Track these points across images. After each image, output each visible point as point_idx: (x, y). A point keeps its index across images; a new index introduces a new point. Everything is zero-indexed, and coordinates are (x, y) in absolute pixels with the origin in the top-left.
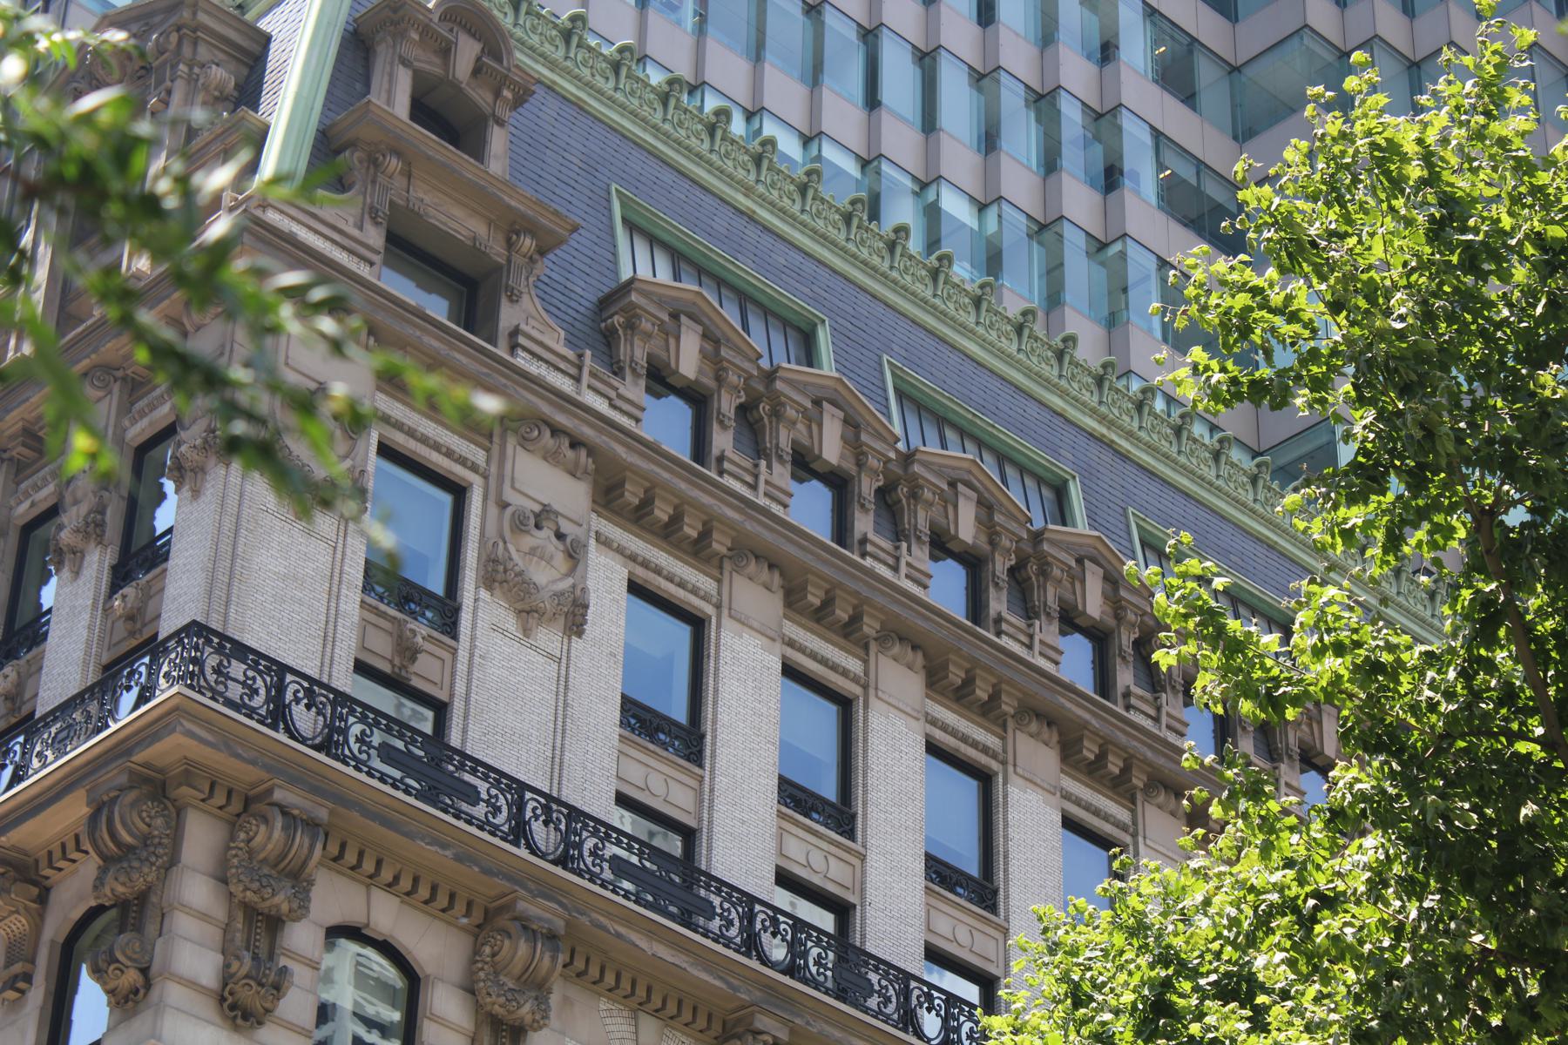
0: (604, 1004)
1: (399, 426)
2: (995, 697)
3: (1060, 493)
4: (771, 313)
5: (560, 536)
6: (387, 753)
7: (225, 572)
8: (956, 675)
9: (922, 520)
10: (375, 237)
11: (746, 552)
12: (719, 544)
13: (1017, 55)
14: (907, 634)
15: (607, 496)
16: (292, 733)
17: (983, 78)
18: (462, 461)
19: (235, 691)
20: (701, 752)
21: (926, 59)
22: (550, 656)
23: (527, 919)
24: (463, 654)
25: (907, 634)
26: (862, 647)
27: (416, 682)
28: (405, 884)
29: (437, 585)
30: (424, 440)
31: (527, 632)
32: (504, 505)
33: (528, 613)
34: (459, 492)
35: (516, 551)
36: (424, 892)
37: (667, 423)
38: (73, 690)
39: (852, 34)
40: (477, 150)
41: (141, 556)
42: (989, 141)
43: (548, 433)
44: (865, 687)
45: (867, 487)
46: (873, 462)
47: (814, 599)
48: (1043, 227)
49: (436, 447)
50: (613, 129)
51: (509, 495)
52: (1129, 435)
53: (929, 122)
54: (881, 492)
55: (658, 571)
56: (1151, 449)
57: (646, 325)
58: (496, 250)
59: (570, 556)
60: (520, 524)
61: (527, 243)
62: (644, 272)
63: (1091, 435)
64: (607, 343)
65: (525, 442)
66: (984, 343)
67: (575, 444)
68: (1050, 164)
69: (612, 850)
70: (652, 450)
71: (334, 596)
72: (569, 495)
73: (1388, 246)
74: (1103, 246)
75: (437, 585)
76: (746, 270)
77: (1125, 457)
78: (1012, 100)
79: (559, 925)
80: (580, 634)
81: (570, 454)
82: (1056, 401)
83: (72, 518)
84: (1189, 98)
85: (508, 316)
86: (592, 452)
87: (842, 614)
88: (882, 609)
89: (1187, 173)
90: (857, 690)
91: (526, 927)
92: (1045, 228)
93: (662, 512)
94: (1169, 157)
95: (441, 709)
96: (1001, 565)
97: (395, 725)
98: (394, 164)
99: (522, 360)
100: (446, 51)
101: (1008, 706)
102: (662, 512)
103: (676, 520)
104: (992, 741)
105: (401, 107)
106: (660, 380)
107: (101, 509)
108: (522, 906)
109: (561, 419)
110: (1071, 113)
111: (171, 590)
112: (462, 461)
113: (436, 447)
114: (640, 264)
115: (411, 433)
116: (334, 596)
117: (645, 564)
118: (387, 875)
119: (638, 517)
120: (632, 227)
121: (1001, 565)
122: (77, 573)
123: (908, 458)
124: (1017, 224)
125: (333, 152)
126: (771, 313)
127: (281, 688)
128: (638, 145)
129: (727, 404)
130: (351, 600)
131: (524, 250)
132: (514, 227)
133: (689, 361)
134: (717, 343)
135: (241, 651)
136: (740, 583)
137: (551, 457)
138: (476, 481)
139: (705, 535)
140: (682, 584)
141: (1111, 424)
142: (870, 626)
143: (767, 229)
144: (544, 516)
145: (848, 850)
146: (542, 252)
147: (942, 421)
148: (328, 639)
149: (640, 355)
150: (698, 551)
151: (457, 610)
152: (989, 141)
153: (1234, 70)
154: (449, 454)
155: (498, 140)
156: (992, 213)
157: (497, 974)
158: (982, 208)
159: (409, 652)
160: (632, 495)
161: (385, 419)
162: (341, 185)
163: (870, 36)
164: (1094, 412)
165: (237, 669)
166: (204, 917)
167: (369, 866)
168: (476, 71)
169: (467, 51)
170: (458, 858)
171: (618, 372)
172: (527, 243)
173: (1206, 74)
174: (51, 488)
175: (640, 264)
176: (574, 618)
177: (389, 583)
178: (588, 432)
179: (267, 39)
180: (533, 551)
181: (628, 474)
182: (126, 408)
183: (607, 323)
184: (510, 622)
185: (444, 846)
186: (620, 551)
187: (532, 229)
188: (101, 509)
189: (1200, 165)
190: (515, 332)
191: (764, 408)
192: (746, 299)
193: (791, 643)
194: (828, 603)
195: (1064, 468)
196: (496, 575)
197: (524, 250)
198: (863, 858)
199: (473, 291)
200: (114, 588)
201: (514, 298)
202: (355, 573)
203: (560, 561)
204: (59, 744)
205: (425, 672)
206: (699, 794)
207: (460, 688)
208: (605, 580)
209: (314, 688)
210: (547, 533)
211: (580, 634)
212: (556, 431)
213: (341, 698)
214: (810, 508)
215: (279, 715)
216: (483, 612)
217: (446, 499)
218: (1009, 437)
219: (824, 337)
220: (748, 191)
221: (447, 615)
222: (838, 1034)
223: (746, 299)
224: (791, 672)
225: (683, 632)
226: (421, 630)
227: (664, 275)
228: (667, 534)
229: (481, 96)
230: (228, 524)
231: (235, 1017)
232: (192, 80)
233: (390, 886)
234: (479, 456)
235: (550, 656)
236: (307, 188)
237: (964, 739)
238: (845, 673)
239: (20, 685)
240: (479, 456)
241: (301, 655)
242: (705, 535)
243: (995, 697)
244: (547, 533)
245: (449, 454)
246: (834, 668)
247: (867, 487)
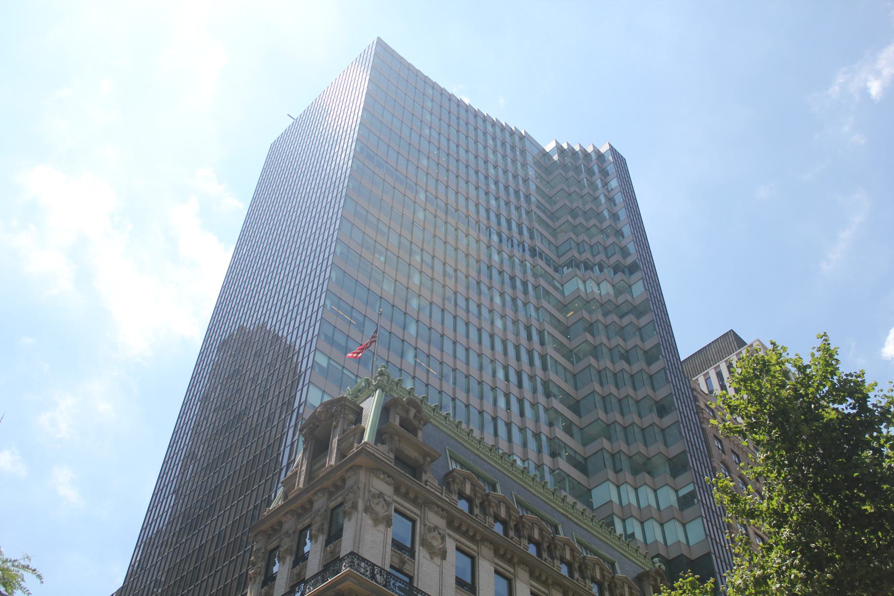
1: (399, 504)
2: (547, 579)
3: (556, 528)
4: (485, 480)
6: (400, 588)
7: (358, 539)
8: (537, 573)
9: (526, 533)
10: (392, 456)
11: (485, 540)
13: (530, 424)
14: (524, 562)
15: (450, 524)
16: (376, 582)
17: (522, 430)
18: (415, 513)
19: (362, 570)
21: (508, 425)
24: (416, 564)
25: (524, 562)
26: (513, 565)
29: (408, 545)
30: (405, 508)
31: (432, 558)
32: (425, 525)
33: (432, 553)
34: (414, 522)
35: (429, 537)
37: (463, 505)
38: (316, 572)
39: (490, 418)
40: (416, 435)
41: (334, 535)
42: (525, 445)
45: (512, 524)
46: (513, 518)
47: (502, 552)
48: (539, 466)
49: (408, 510)
50: (445, 433)
51: (427, 522)
52: (571, 514)
53: (510, 440)
54: (515, 526)
55: (463, 544)
56: (577, 518)
57: (457, 481)
58: (421, 460)
61: (429, 459)
62: (454, 467)
63: (562, 514)
64: (448, 485)
65: (430, 509)
66: (535, 490)
67: (443, 510)
68: (540, 451)
70: (461, 511)
71: (385, 547)
72: (441, 523)
73: (822, 362)
74: (554, 471)
75: (408, 545)
76: (479, 469)
77: (570, 519)
78: (529, 435)
82: (554, 505)
83: (315, 528)
84: (572, 436)
85: (424, 477)
87: (509, 557)
89: (572, 454)
92: (539, 467)
93: (464, 528)
94: (568, 449)
95: (411, 578)
96: (545, 545)
97: (401, 580)
98: (397, 438)
99: (428, 487)
100: (407, 411)
101: (550, 582)
102: (464, 528)
103: (467, 530)
104: (546, 591)
105: (397, 423)
106: (461, 495)
107: (323, 525)
109: (439, 503)
110: (543, 438)
111: (343, 545)
112: (415, 513)
113: (408, 510)
114: (453, 466)
115: (402, 506)
116: (385, 547)
117: (460, 542)
119: (458, 530)
120: (451, 457)
121: (545, 545)
122: (316, 542)
123: (521, 517)
124: (532, 467)
125: (380, 436)
126: (485, 480)
127: (374, 570)
128: (452, 437)
129: (478, 501)
130: (389, 548)
132: (425, 455)
133: (468, 490)
135: (364, 560)
136: (483, 548)
137: (437, 513)
138: (418, 519)
139: (475, 535)
140: (469, 547)
141: (567, 511)
142: (515, 560)
143: (483, 459)
144: (436, 528)
146: (432, 461)
147: (527, 509)
148: (383, 558)
149: (456, 489)
150: (472, 539)
151: (414, 552)
152: (525, 445)
153: (582, 429)
154: (412, 511)
155: (420, 433)
156: (526, 463)
158: (524, 461)
159: (403, 562)
160: (456, 524)
161: (396, 502)
162: (383, 443)
163: (495, 419)
164: (562, 508)
165: (363, 564)
168: (415, 416)
169: (413, 412)
171: (451, 492)
172: (429, 459)
173: (575, 430)
174: (309, 520)
175: (453, 466)
176: (443, 555)
177: (396, 544)
178: (446, 507)
179: (362, 409)
180: (433, 537)
182: (329, 499)
183: (448, 480)
184: (428, 556)
186: (454, 538)
187: (430, 455)
188: (323, 525)
189: (575, 452)
190: (427, 481)
191: (486, 503)
192: (478, 476)
193: (496, 564)
194: (505, 553)
195: (557, 521)
196: (424, 543)
199: (415, 470)
200: (326, 545)
201: (426, 473)
202: (390, 541)
203: (439, 539)
204: (314, 586)
205: (407, 568)
207: (416, 573)
208: (450, 545)
209: (382, 570)
210: (436, 533)
212: (438, 506)
213: (388, 573)
214: (498, 528)
215: (373, 577)
216: (421, 553)
217: (410, 524)
218: (543, 513)
219: (498, 487)
220: (478, 450)
221: (412, 553)
223: (478, 476)
224: (497, 572)
225: (468, 561)
226: (406, 557)
227: (459, 468)
228: (465, 534)
229: (416, 423)
230: (358, 527)
232: (344, 418)
234: (419, 512)
236: (376, 444)
237: (539, 590)
238: (509, 572)
239: (300, 572)
240: (419, 512)
241: (377, 561)
242: (475, 535)
243: (547, 579)
244: (436, 533)
245: (412, 511)
246: (507, 570)
247: (512, 524)
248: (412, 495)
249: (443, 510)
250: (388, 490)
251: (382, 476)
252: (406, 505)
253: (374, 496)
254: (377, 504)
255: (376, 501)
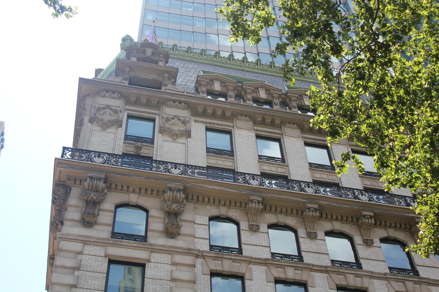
0: (208, 207)
5: (179, 120)
12: (228, 114)
18: (152, 113)
20: (233, 155)
22: (183, 143)
23: (171, 187)
27: (142, 154)
28: (137, 190)
31: (174, 140)
32: (163, 118)
36: (143, 191)
43: (172, 102)
44: (282, 135)
51: (164, 116)
55: (214, 124)
58: (160, 79)
59: (183, 123)
60: (168, 120)
65: (167, 106)
67: (180, 103)
69: (196, 171)
79: (182, 187)
80: (190, 137)
81: (180, 105)
86: (185, 103)
87: (268, 120)
88: (278, 117)
90: (280, 136)
91: (171, 189)
100: (144, 52)
108: (168, 185)
112: (152, 113)
118: (131, 189)
119: (204, 114)
131: (166, 77)
134: (225, 83)
145: (283, 165)
154: (148, 113)
157: (166, 202)
160: (200, 110)
166: (76, 206)
167: (125, 188)
170: (146, 178)
176: (188, 134)
180: (172, 124)
181: (198, 106)
185: (141, 176)
186: (202, 122)
196: (162, 131)
197: (166, 77)
198: (288, 166)
206: (234, 162)
207: (155, 153)
211: (190, 137)
222: (277, 196)
228: (214, 115)
231: (85, 225)
233: (134, 192)
235: (183, 143)
245: (148, 113)
248: (144, 101)
249: (180, 103)
250: (117, 103)
251: (107, 94)
252: (143, 110)
253: (99, 109)
254: (103, 114)
255: (102, 112)
